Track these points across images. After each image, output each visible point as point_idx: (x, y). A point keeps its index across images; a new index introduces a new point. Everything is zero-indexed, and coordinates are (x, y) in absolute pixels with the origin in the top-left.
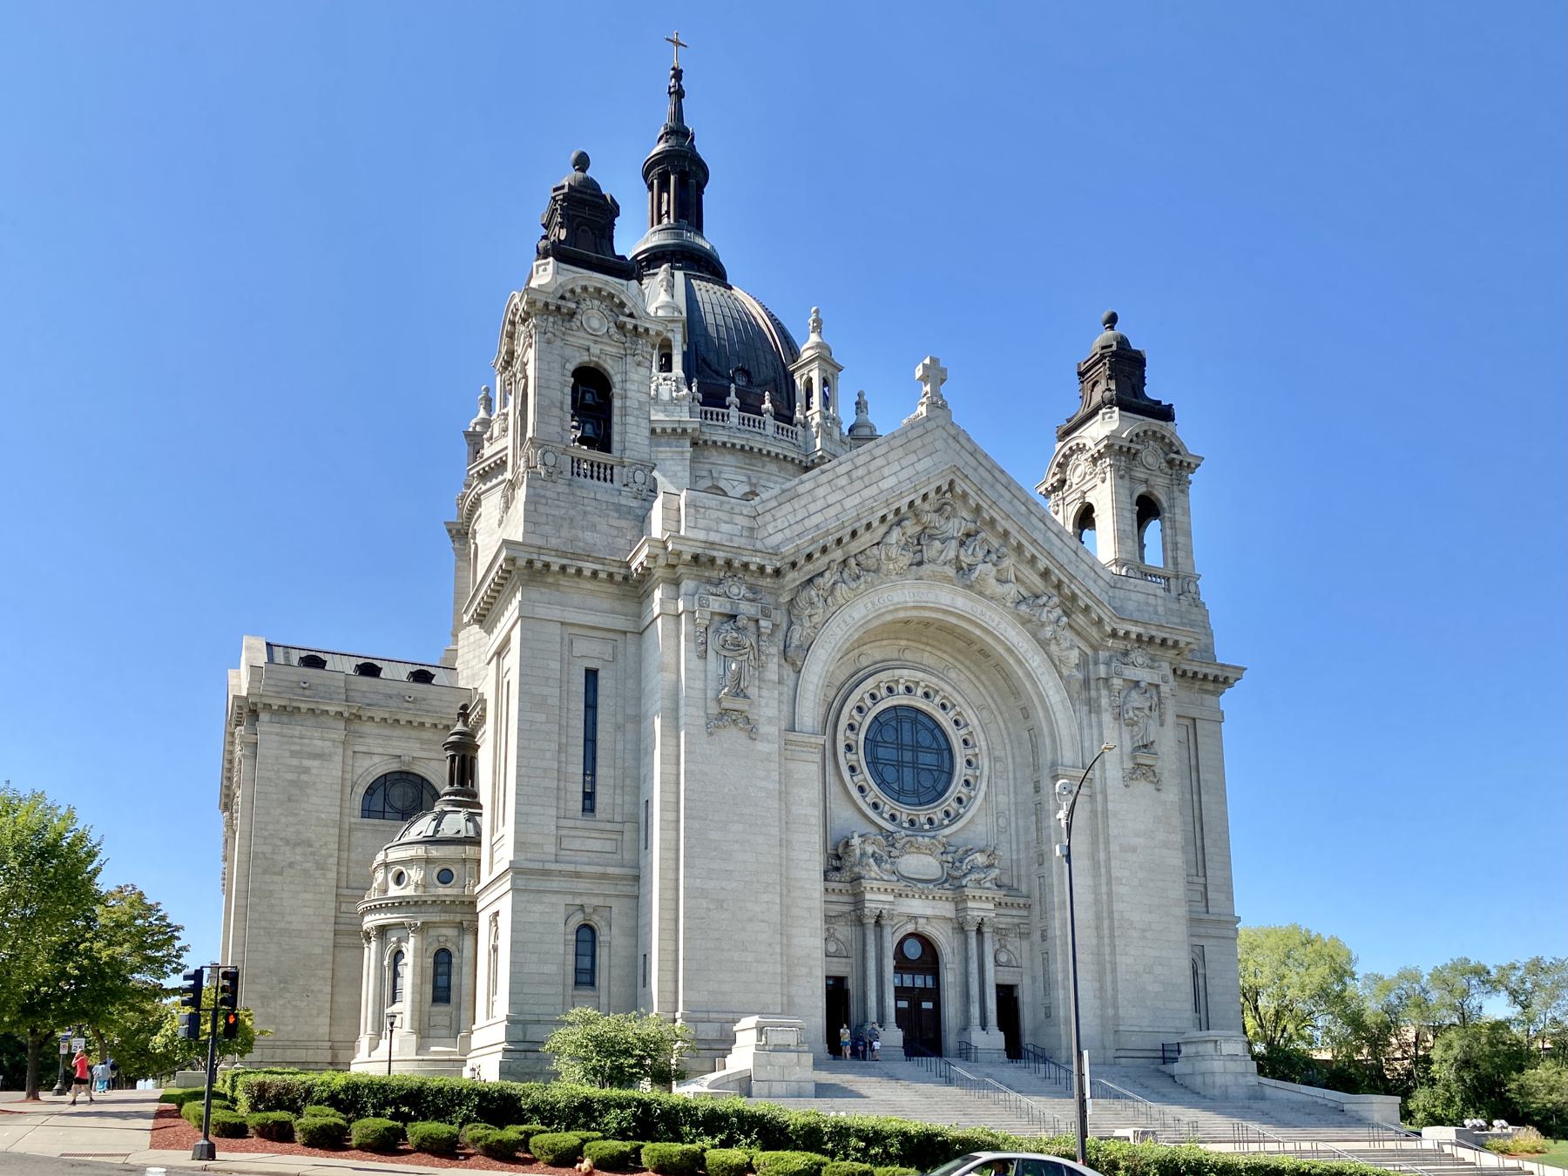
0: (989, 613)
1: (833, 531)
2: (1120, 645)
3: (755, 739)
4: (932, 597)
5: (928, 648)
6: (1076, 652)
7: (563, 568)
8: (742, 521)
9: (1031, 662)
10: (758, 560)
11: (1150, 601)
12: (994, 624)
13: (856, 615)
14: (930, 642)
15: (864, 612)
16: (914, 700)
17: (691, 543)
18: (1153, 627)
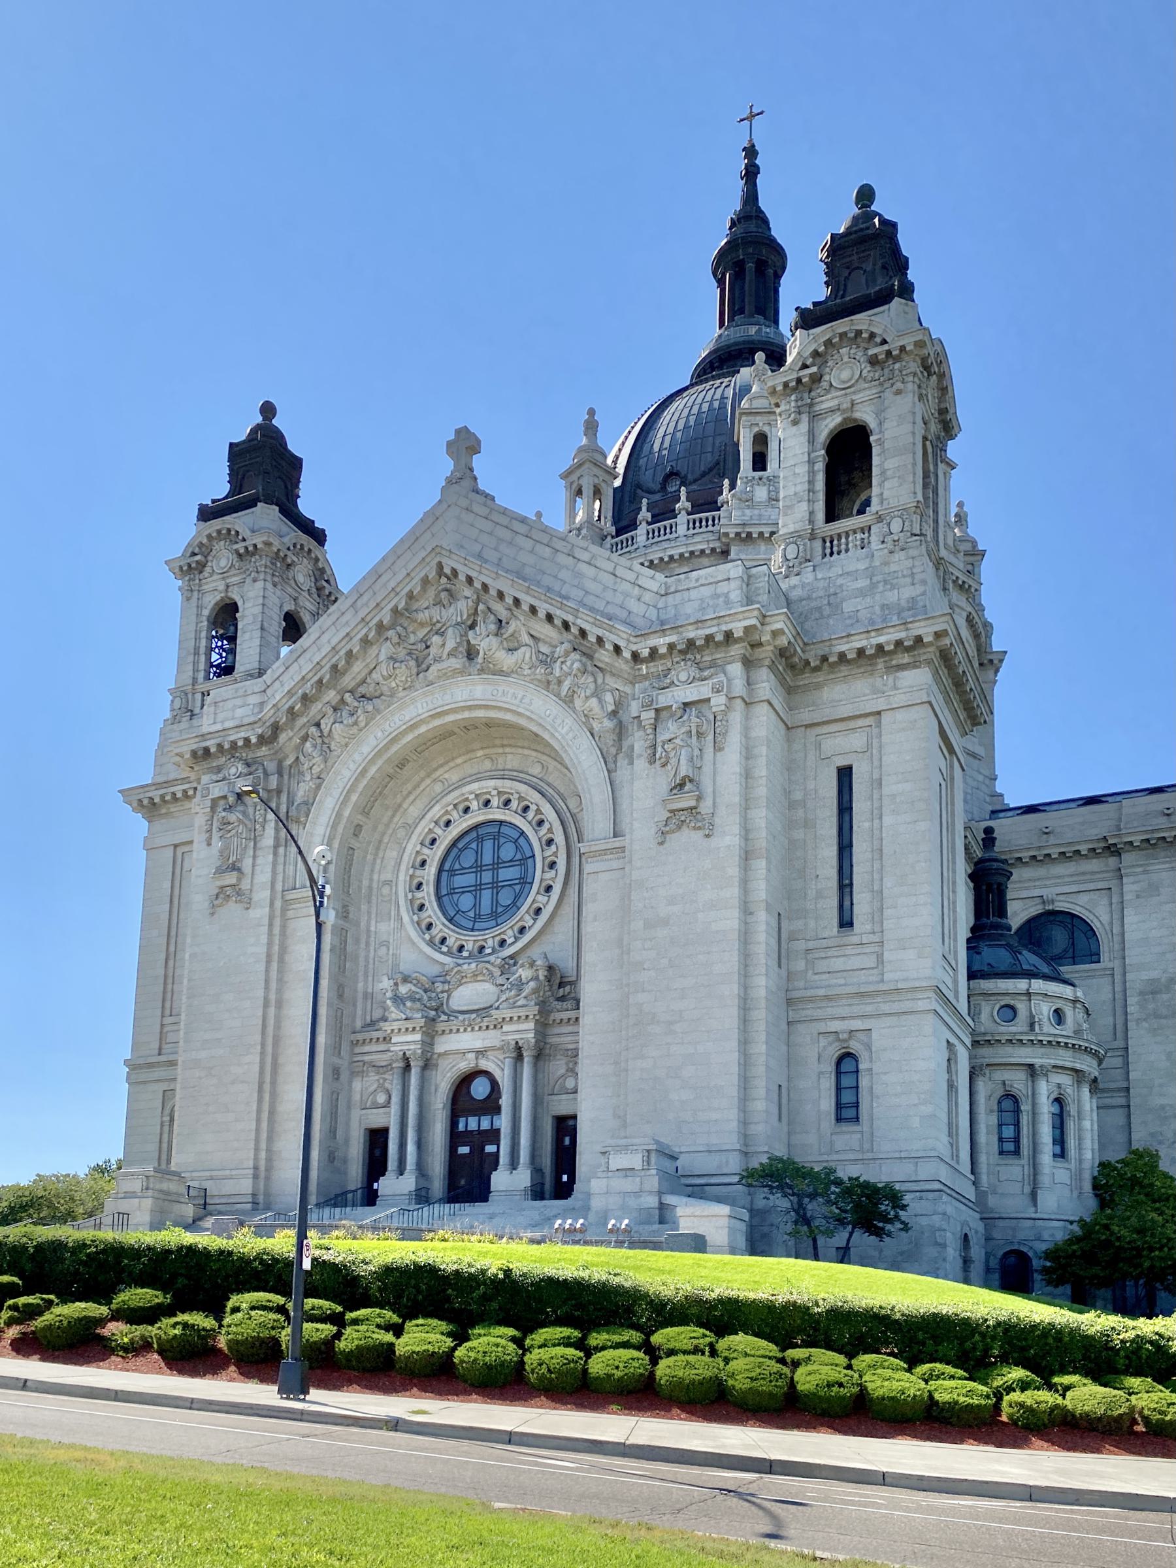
0: (512, 691)
1: (311, 675)
2: (657, 667)
3: (248, 909)
4: (448, 699)
5: (508, 750)
6: (608, 698)
7: (162, 797)
8: (254, 699)
9: (560, 729)
10: (243, 735)
11: (719, 591)
12: (517, 702)
13: (366, 749)
14: (505, 742)
15: (373, 742)
16: (476, 816)
17: (188, 742)
18: (690, 627)
